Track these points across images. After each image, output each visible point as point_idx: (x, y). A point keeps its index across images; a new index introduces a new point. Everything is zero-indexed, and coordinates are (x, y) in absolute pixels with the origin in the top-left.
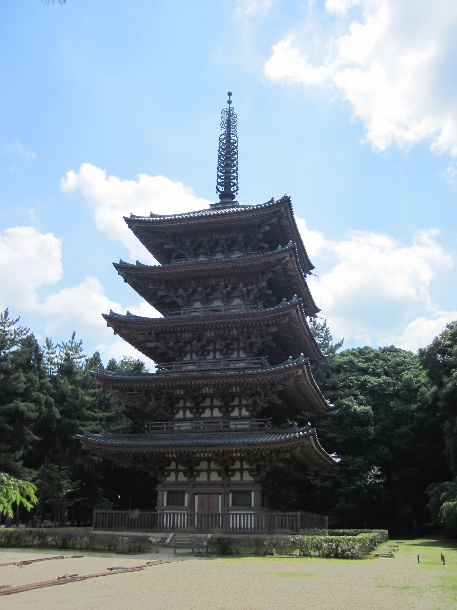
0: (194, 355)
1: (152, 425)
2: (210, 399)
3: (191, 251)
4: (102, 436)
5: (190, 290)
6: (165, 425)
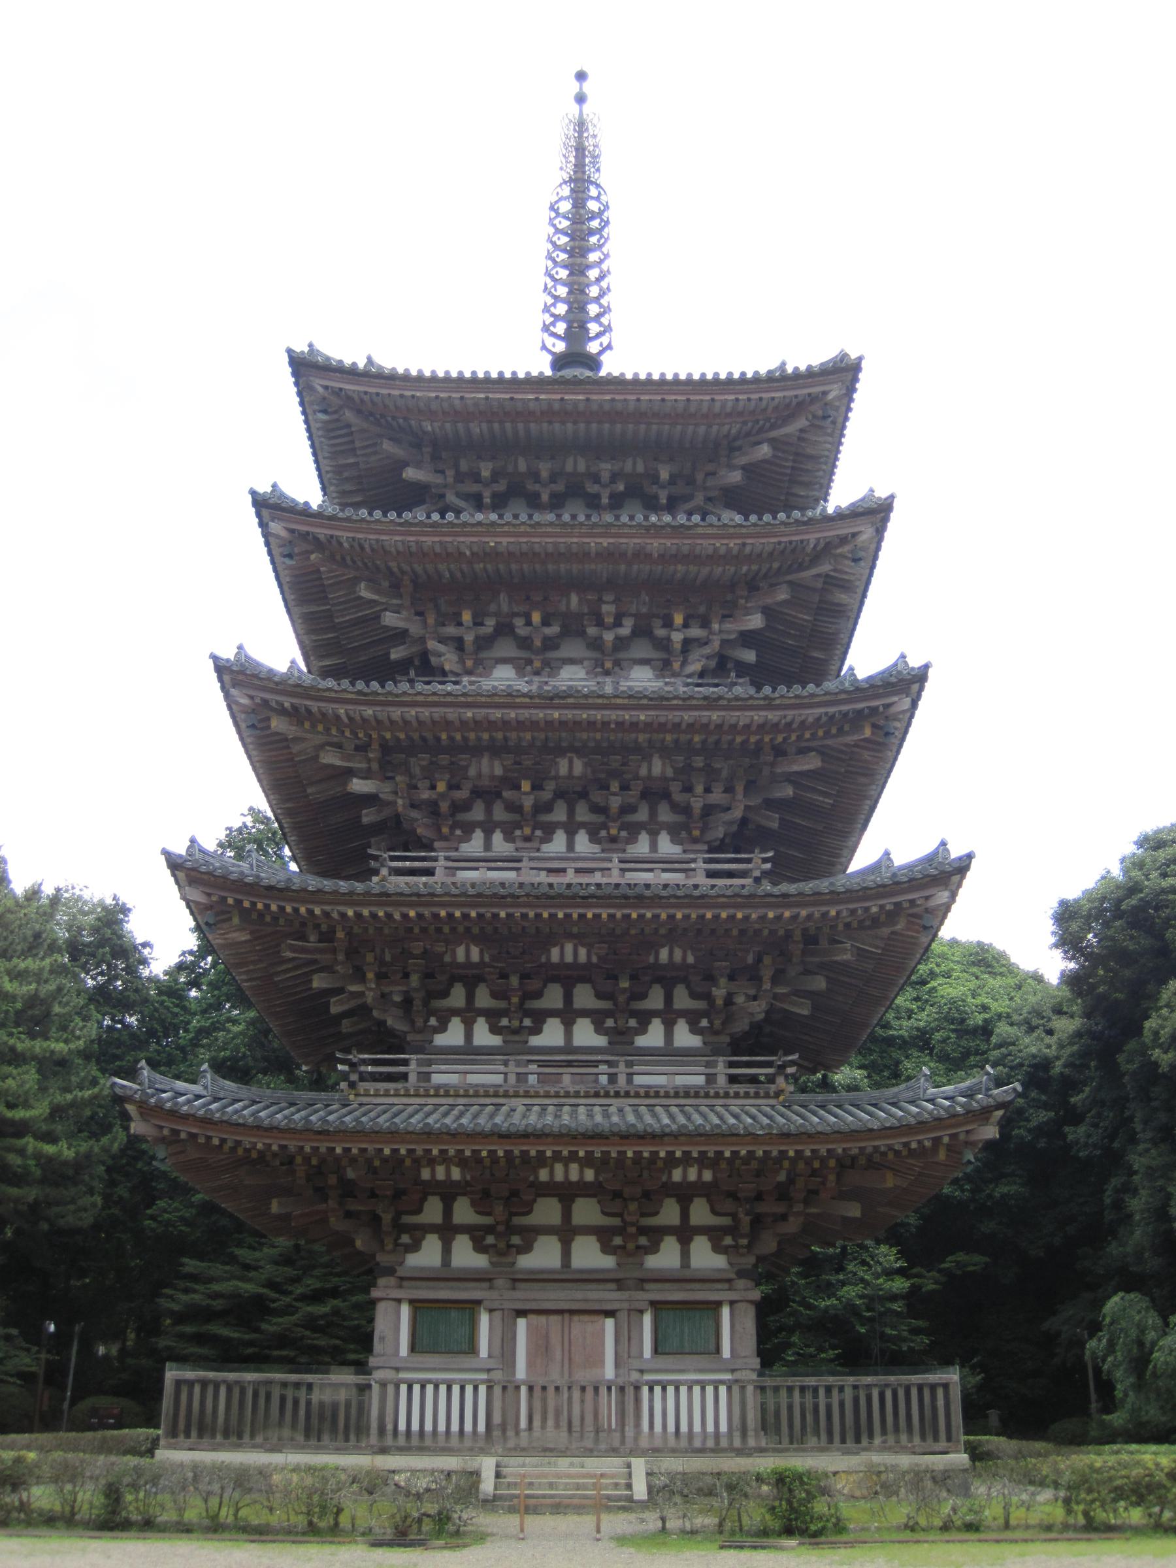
0: (498, 837)
1: (365, 1062)
2: (563, 986)
3: (487, 500)
4: (204, 1093)
5: (490, 623)
6: (413, 1066)
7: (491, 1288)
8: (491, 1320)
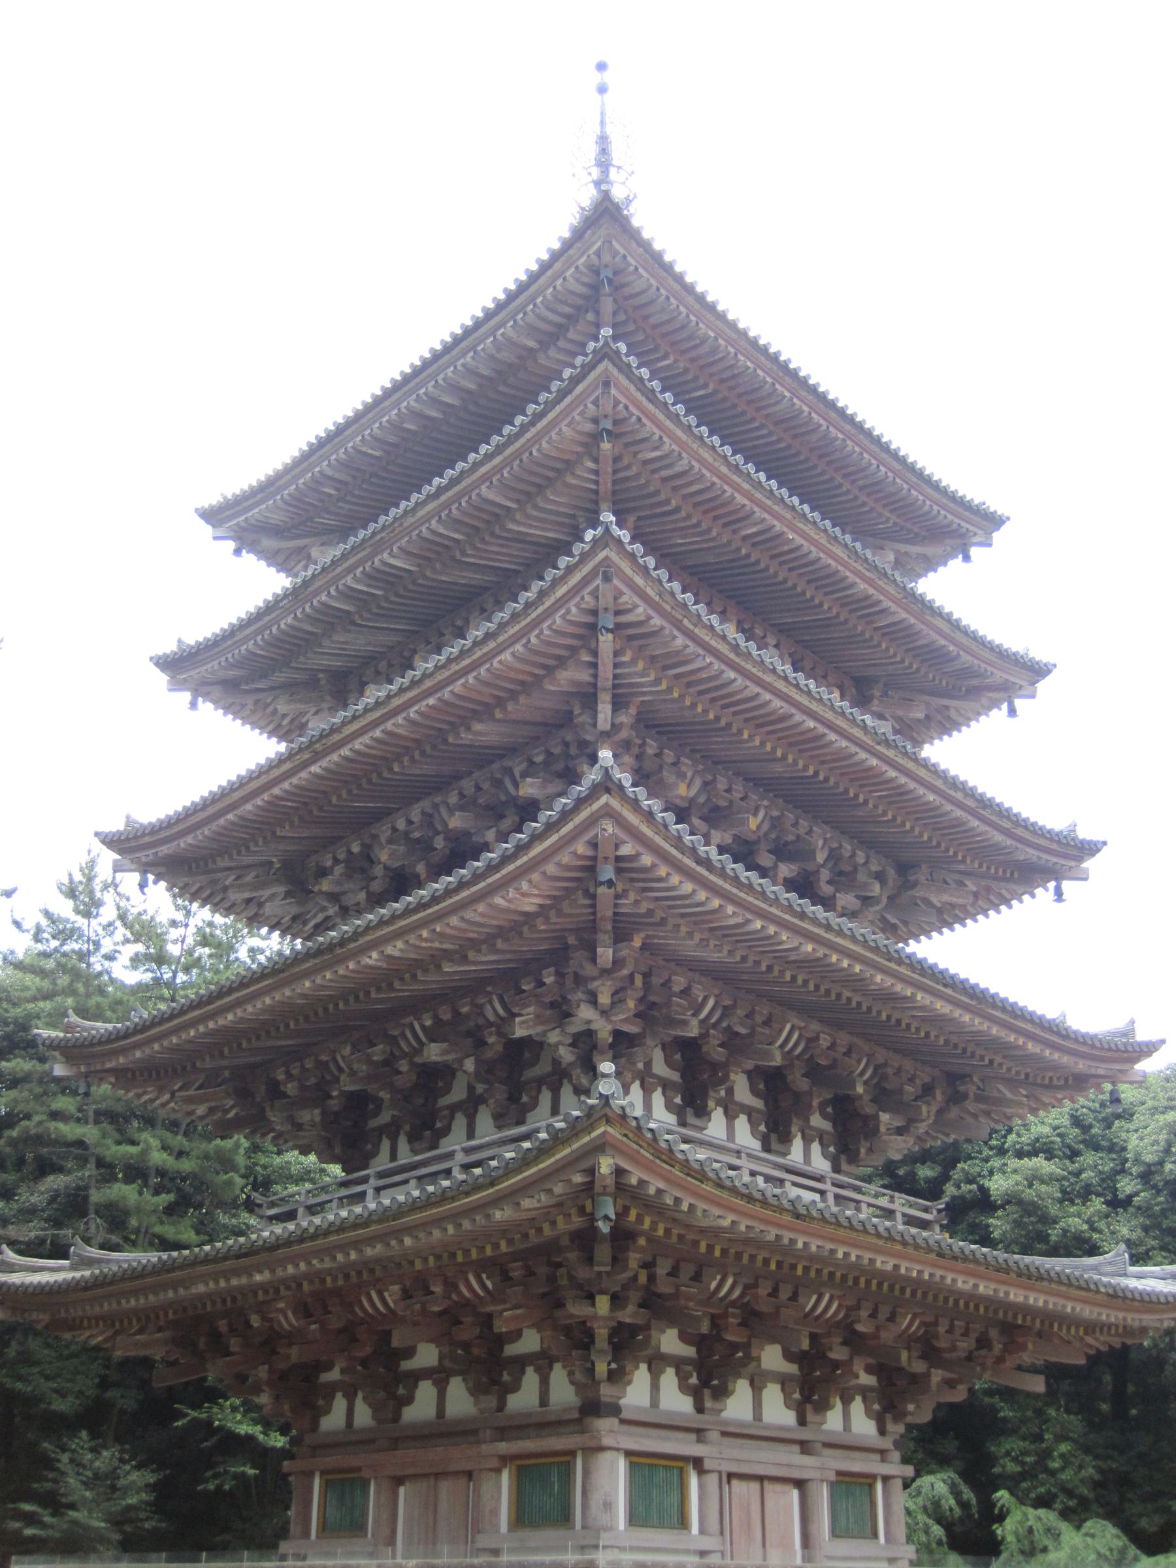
7: (699, 1441)
8: (701, 1486)
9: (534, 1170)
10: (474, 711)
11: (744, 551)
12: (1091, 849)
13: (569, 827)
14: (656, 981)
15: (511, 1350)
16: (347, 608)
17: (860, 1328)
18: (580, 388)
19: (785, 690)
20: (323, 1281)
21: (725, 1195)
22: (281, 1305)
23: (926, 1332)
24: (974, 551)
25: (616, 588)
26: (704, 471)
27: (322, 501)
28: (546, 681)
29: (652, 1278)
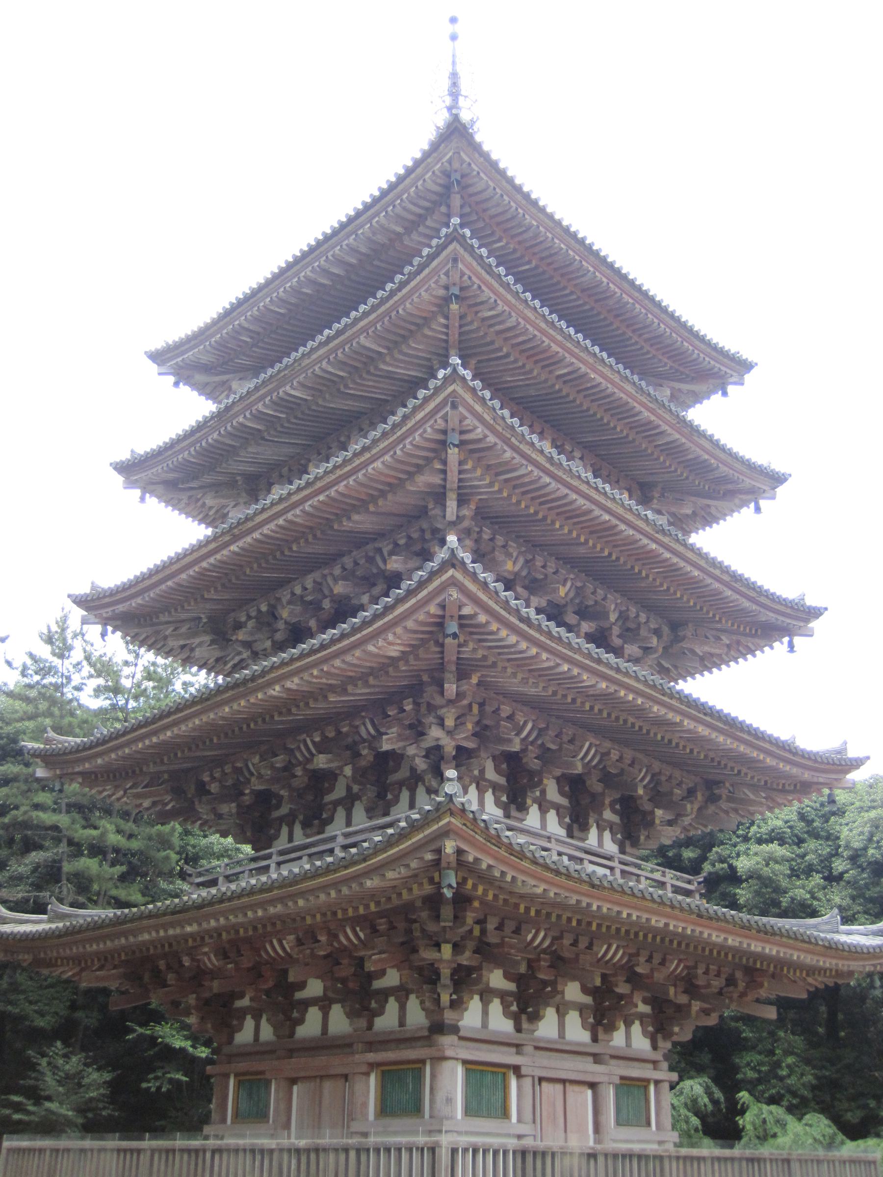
7: (518, 1053)
9: (396, 850)
10: (354, 506)
11: (557, 387)
12: (815, 613)
13: (424, 593)
14: (489, 709)
15: (378, 984)
16: (259, 427)
17: (639, 970)
18: (435, 263)
19: (587, 491)
20: (237, 932)
21: (539, 870)
22: (206, 949)
23: (688, 974)
24: (730, 389)
25: (461, 413)
26: (528, 326)
27: (240, 346)
28: (407, 483)
29: (483, 932)
